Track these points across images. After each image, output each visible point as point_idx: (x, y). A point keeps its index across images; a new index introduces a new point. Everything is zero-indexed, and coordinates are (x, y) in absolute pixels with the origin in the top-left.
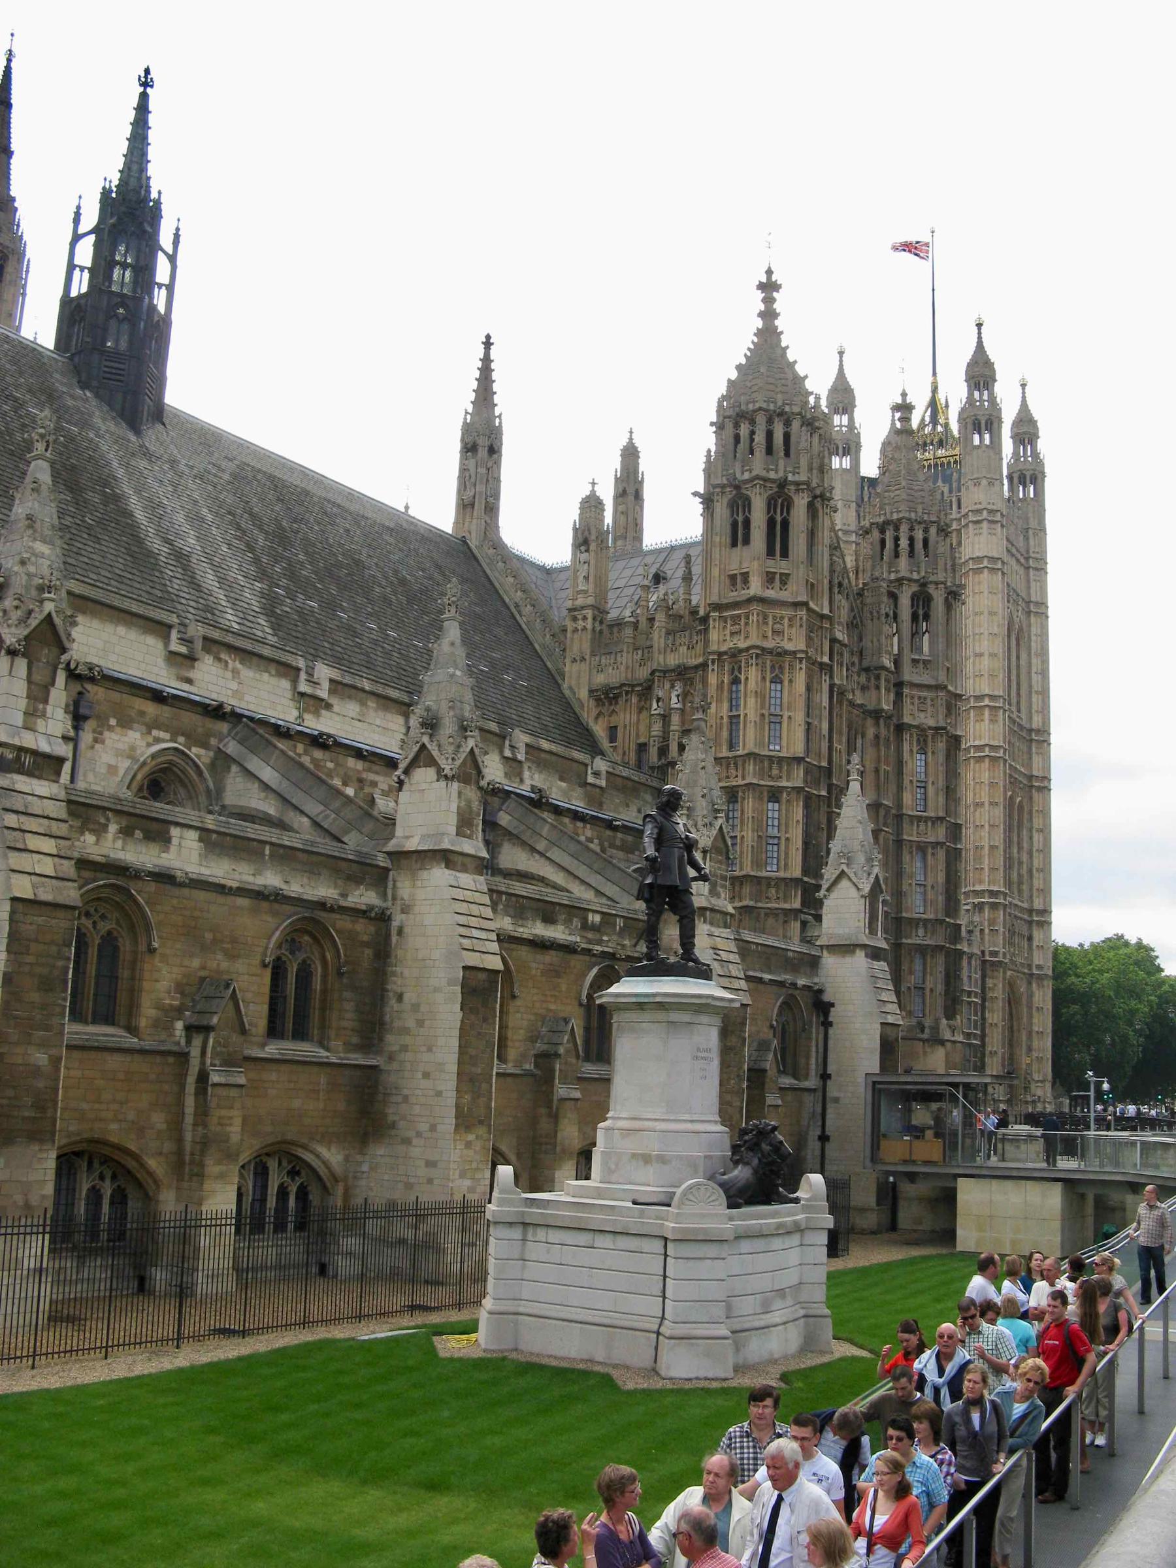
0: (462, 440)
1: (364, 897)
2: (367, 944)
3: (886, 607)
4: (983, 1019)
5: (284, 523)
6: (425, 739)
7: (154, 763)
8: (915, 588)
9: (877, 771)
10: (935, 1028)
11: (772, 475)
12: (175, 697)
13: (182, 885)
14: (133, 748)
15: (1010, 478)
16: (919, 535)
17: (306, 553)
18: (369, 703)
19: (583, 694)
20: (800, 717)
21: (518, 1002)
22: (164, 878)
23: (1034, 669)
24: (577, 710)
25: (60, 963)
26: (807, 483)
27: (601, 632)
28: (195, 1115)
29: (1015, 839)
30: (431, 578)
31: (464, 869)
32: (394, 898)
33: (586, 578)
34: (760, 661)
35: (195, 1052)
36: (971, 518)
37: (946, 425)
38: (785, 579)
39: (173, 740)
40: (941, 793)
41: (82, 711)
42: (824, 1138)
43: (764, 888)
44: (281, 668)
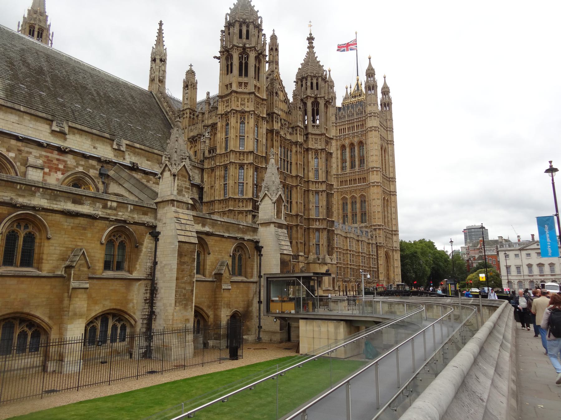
4: (378, 263)
5: (45, 68)
8: (313, 100)
9: (297, 164)
10: (324, 259)
15: (381, 105)
16: (315, 81)
17: (52, 79)
18: (25, 117)
21: (51, 241)
23: (390, 160)
26: (254, 47)
27: (193, 119)
29: (386, 210)
30: (125, 99)
36: (369, 115)
38: (246, 84)
40: (324, 172)
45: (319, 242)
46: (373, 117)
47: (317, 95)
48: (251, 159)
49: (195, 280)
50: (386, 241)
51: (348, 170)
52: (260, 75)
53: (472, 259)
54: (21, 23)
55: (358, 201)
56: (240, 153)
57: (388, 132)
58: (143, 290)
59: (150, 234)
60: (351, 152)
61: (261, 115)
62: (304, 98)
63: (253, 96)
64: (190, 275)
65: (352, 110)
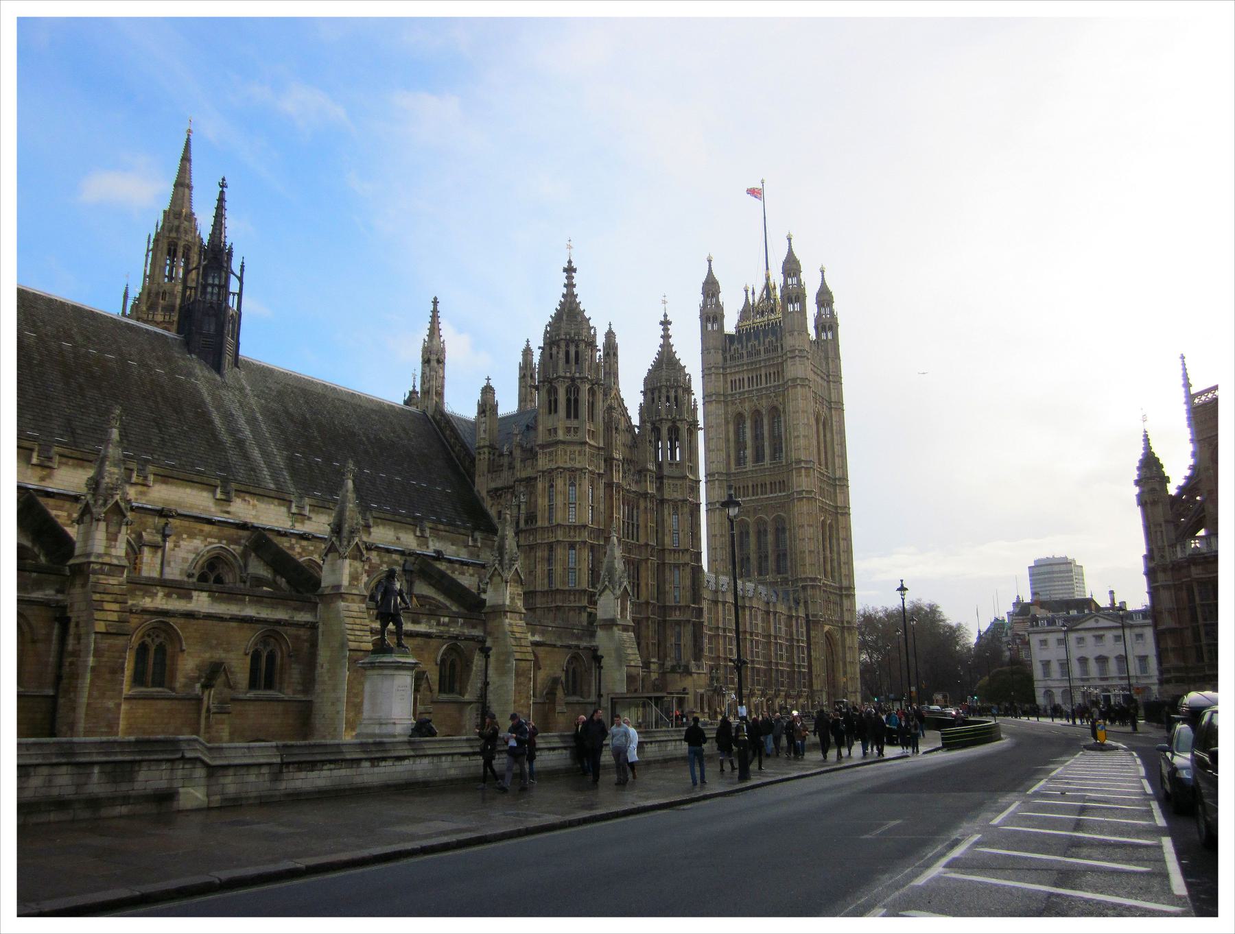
0: (423, 357)
1: (304, 617)
2: (306, 641)
4: (809, 656)
8: (670, 424)
9: (646, 527)
11: (568, 375)
12: (219, 521)
14: (196, 549)
15: (816, 328)
16: (672, 394)
22: (190, 615)
23: (835, 443)
28: (205, 728)
29: (828, 546)
30: (398, 436)
31: (353, 601)
33: (485, 431)
34: (563, 475)
35: (205, 698)
38: (576, 430)
39: (220, 542)
41: (167, 532)
44: (281, 502)
45: (680, 641)
46: (797, 358)
51: (749, 465)
52: (594, 412)
53: (1018, 641)
54: (153, 237)
55: (770, 529)
56: (569, 527)
60: (756, 428)
62: (656, 421)
64: (527, 697)
65: (756, 343)
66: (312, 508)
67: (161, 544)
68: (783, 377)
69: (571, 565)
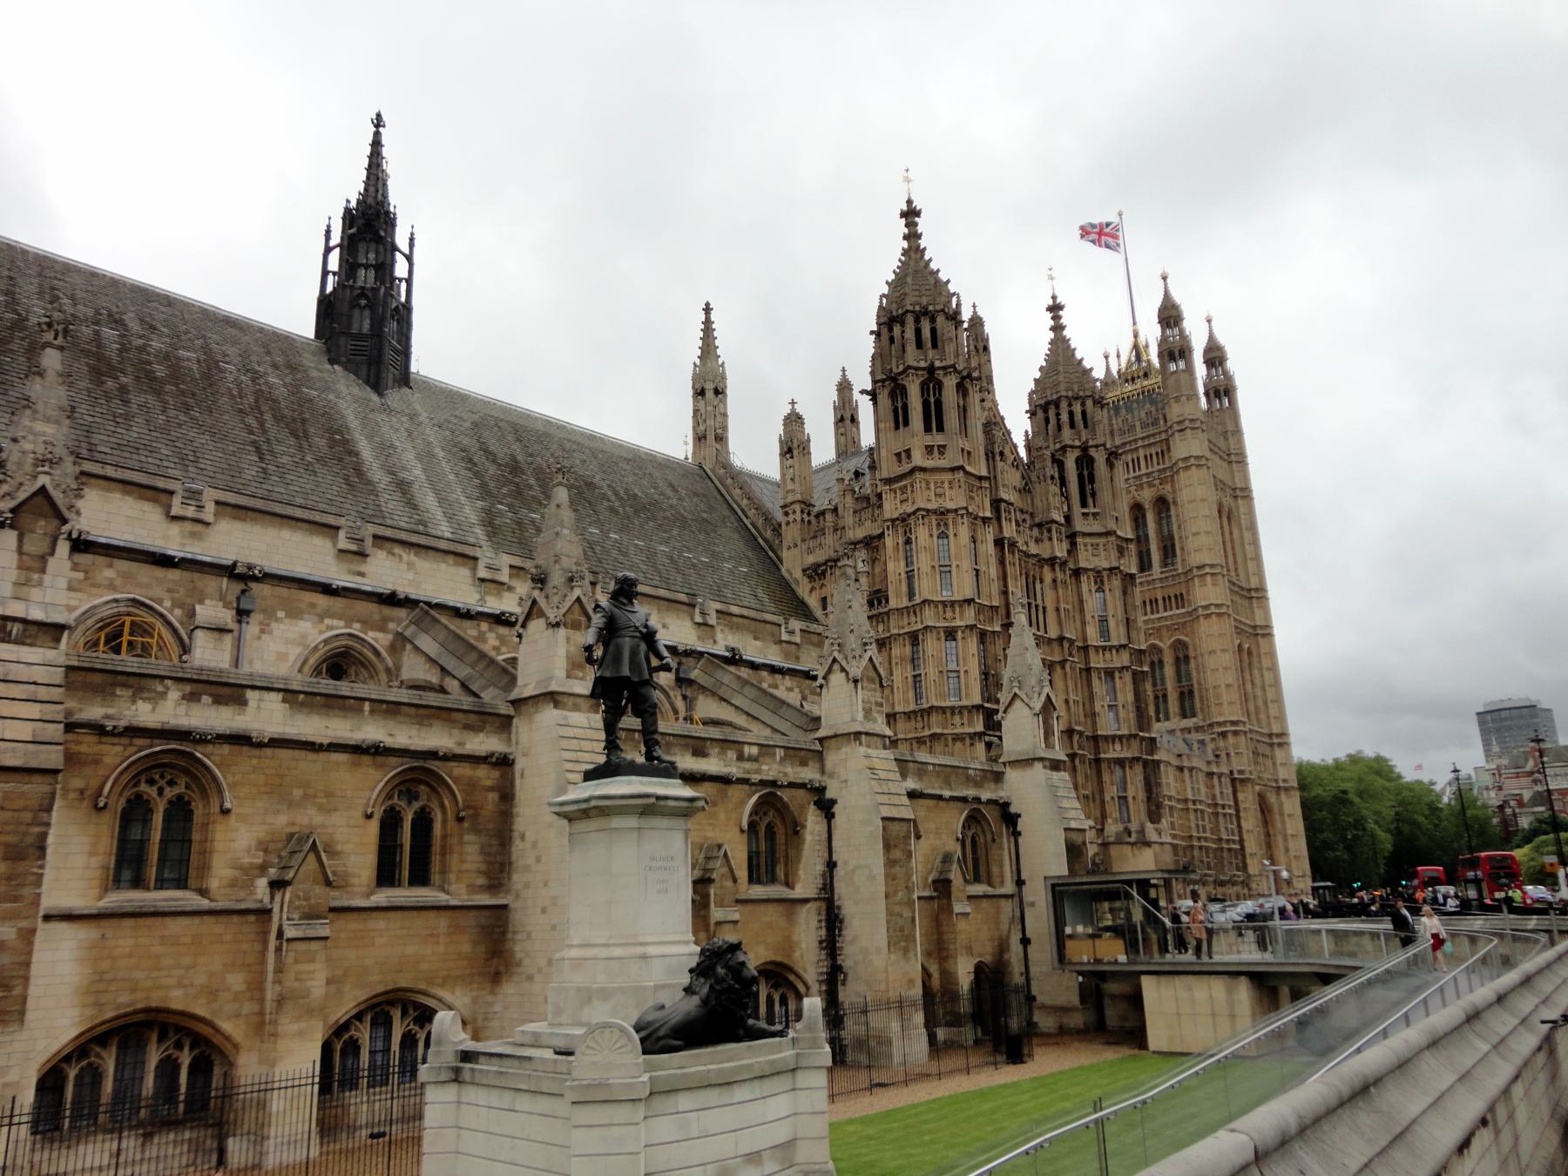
1: (484, 743)
2: (491, 789)
3: (1052, 470)
4: (1239, 826)
5: (519, 458)
6: (536, 594)
7: (327, 648)
8: (1077, 453)
9: (1058, 609)
10: (1142, 832)
11: (923, 364)
13: (260, 745)
14: (304, 637)
15: (1207, 394)
16: (1077, 408)
19: (798, 574)
20: (966, 564)
22: (240, 740)
23: (1246, 542)
24: (794, 586)
25: (37, 830)
26: (953, 366)
27: (809, 522)
28: (275, 972)
30: (662, 494)
31: (576, 708)
32: (517, 743)
33: (792, 480)
34: (926, 520)
35: (276, 909)
36: (1176, 427)
37: (1149, 361)
42: (1025, 941)
43: (948, 714)
46: (1188, 431)
47: (1087, 441)
48: (969, 616)
49: (915, 896)
50: (1256, 763)
52: (968, 423)
55: (1168, 659)
56: (943, 603)
57: (1234, 465)
58: (814, 923)
59: (815, 804)
61: (981, 514)
63: (961, 474)
64: (907, 887)
65: (1129, 417)
66: (515, 571)
67: (232, 625)
68: (1170, 457)
69: (952, 666)
